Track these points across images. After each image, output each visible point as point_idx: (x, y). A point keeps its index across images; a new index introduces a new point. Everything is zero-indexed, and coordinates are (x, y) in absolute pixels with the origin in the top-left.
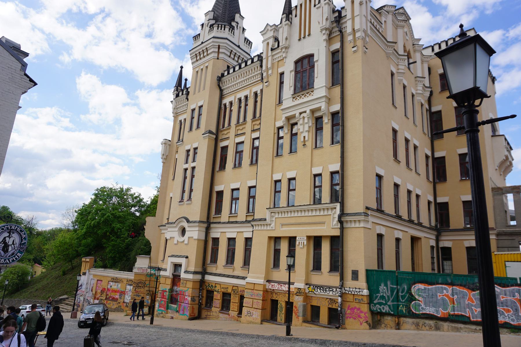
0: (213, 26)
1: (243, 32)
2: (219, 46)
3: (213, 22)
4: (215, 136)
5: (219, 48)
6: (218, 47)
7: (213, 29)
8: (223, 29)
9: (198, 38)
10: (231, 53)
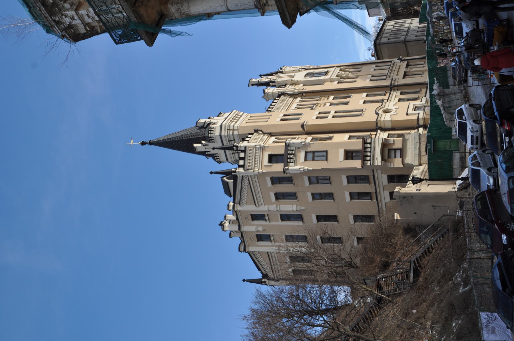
0: (209, 138)
2: (228, 130)
5: (230, 130)
6: (228, 131)
7: (213, 137)
8: (212, 129)
9: (217, 155)
10: (233, 122)
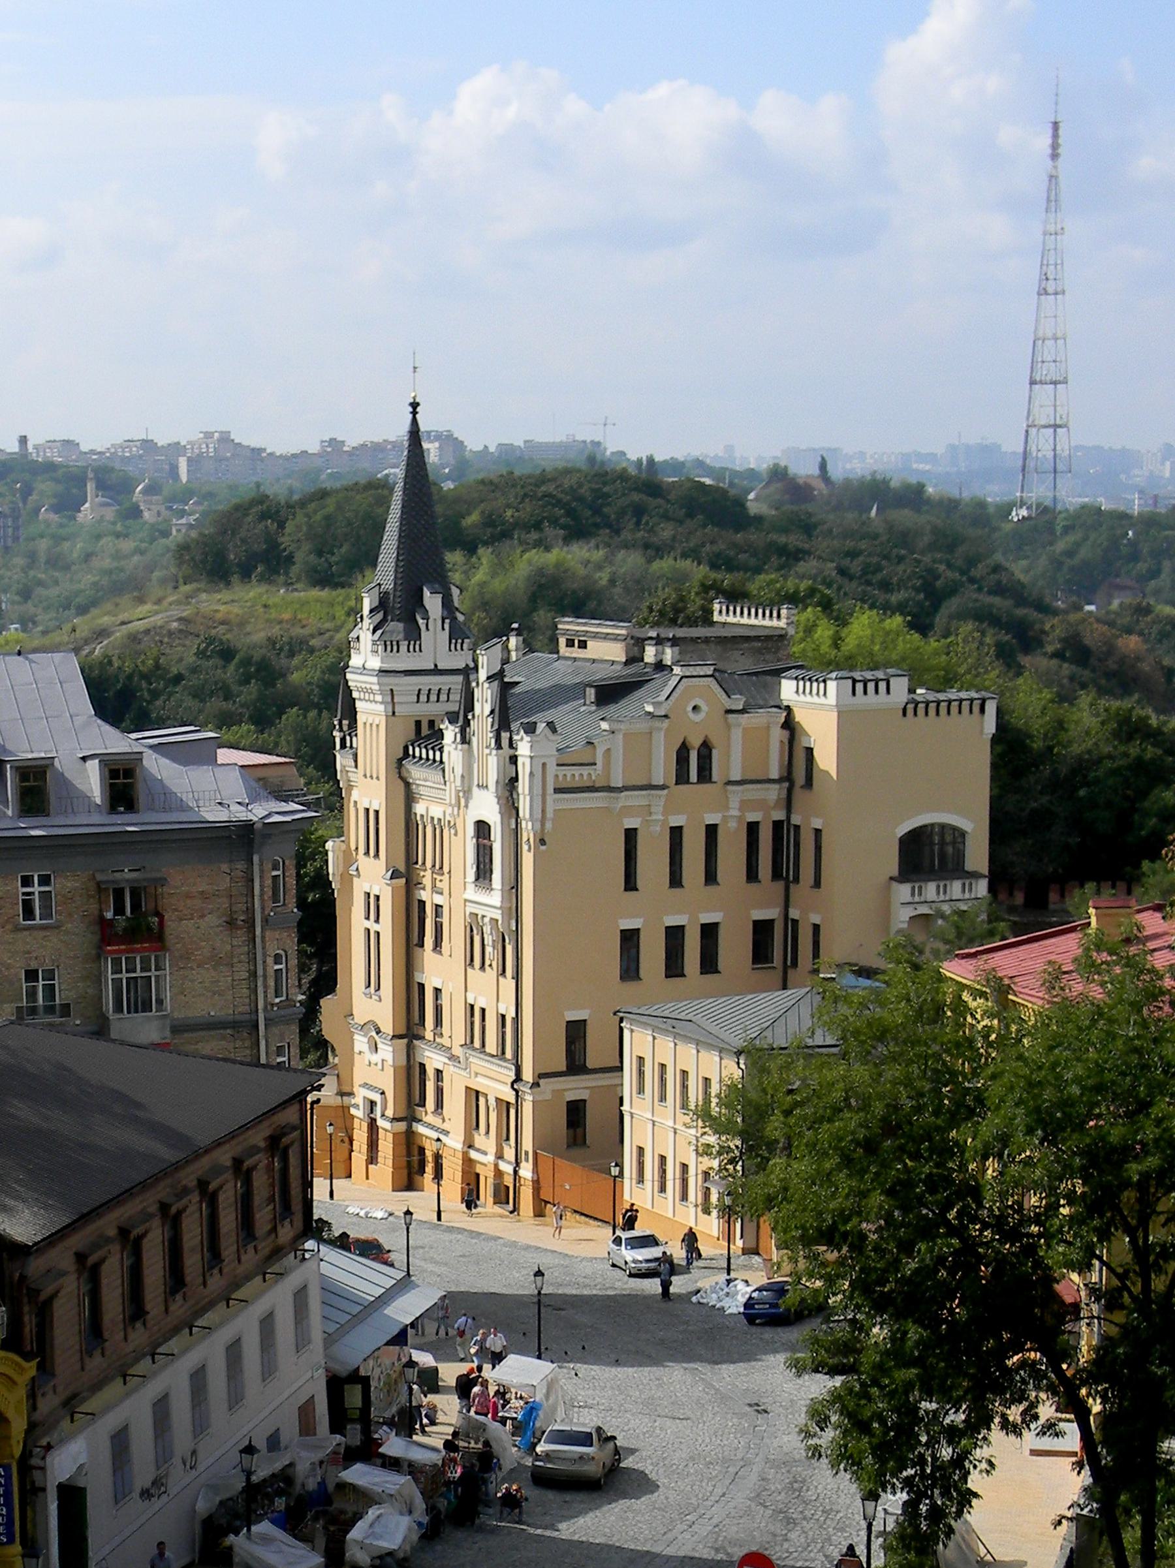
1: (443, 629)
3: (380, 616)
4: (404, 880)
8: (395, 648)
